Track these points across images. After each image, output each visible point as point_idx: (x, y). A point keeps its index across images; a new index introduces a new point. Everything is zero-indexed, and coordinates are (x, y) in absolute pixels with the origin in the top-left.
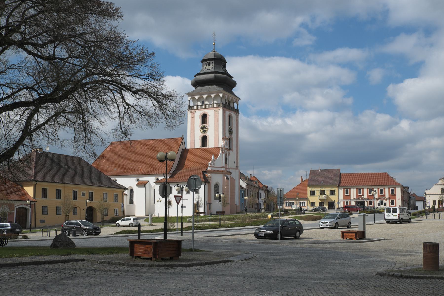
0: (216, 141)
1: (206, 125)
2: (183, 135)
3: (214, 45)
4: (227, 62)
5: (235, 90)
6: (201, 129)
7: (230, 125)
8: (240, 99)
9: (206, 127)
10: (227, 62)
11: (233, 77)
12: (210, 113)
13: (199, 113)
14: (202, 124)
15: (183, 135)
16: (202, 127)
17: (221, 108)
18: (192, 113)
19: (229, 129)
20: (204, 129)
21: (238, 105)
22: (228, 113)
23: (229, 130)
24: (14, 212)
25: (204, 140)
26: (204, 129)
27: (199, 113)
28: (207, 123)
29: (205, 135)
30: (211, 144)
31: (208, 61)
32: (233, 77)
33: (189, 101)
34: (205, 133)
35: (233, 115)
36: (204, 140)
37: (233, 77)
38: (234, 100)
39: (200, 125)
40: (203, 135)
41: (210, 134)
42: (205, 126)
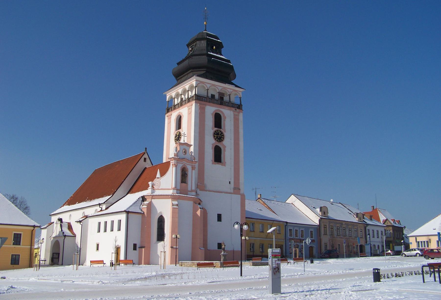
9: (222, 133)
16: (215, 132)
24: (360, 253)
28: (221, 128)
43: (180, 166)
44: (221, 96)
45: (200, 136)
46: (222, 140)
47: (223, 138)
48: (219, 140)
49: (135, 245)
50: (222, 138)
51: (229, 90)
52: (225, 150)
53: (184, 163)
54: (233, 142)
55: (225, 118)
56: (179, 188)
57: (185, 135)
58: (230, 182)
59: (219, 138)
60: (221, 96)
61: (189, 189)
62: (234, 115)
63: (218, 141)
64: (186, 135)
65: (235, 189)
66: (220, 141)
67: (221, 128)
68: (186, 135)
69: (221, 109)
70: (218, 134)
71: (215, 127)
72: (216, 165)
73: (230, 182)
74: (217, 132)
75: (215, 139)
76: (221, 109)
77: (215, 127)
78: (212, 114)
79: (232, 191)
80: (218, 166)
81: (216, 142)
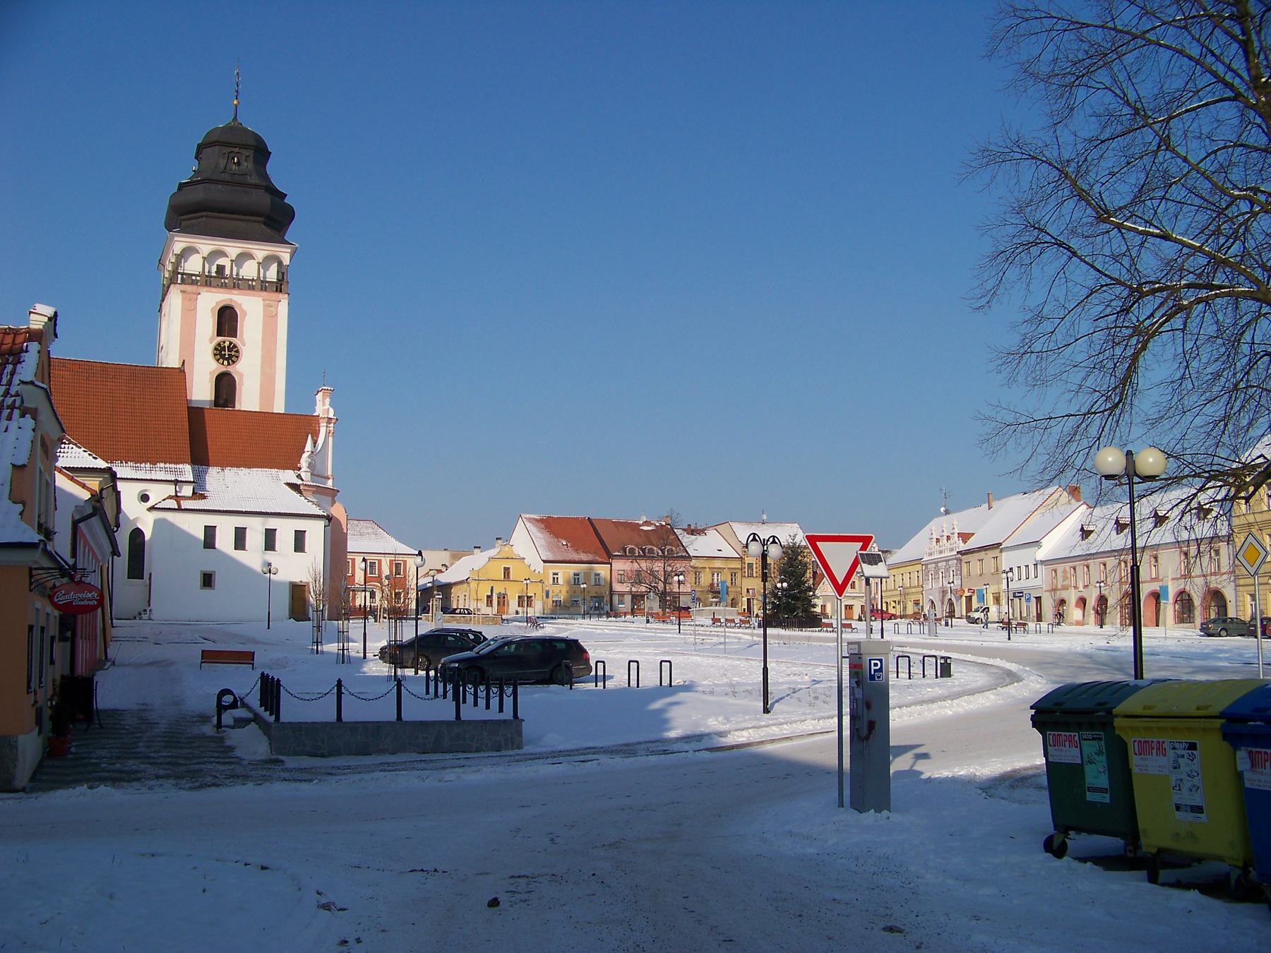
0: (267, 389)
2: (184, 362)
6: (216, 349)
9: (235, 346)
12: (250, 307)
13: (210, 301)
15: (184, 362)
18: (185, 295)
20: (227, 354)
25: (225, 387)
26: (227, 354)
27: (210, 301)
29: (230, 369)
30: (248, 399)
31: (233, 149)
34: (229, 364)
36: (225, 387)
39: (211, 341)
40: (223, 369)
41: (247, 371)
42: (231, 343)
46: (234, 362)
47: (237, 357)
48: (226, 362)
52: (241, 380)
55: (245, 314)
59: (227, 356)
62: (266, 306)
66: (229, 364)
71: (219, 335)
75: (218, 360)
77: (219, 335)
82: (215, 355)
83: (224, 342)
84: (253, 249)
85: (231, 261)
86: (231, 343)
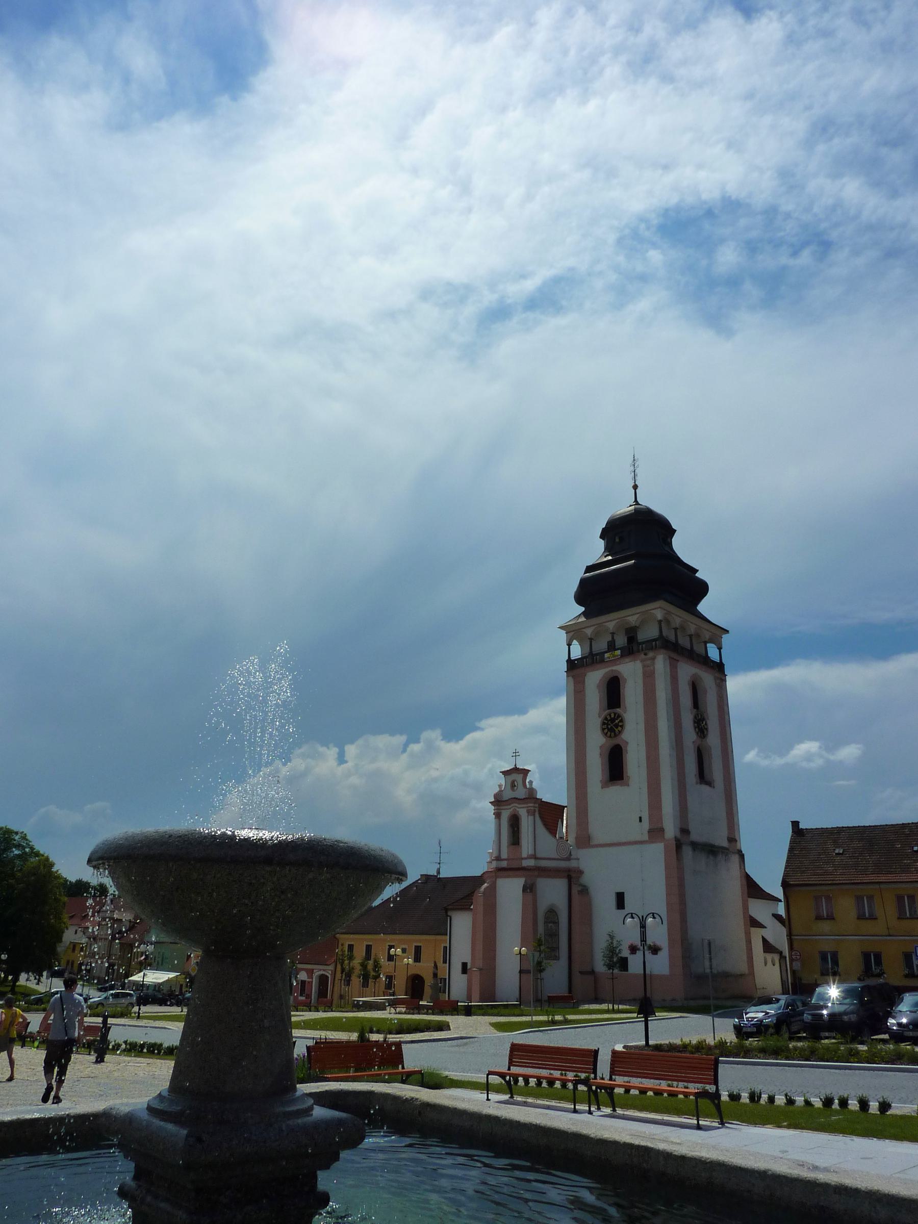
1: (618, 709)
3: (635, 487)
4: (676, 531)
5: (704, 607)
6: (604, 724)
7: (696, 704)
8: (727, 632)
9: (619, 716)
10: (676, 531)
11: (697, 571)
13: (595, 678)
14: (609, 709)
16: (606, 719)
17: (662, 651)
19: (695, 717)
21: (720, 649)
22: (687, 671)
23: (695, 722)
28: (619, 706)
32: (698, 571)
33: (569, 645)
35: (707, 679)
37: (697, 571)
38: (707, 635)
43: (506, 815)
44: (631, 633)
45: (576, 739)
49: (464, 965)
50: (619, 727)
51: (630, 619)
53: (513, 807)
54: (642, 726)
56: (504, 855)
57: (517, 754)
58: (640, 818)
60: (631, 633)
61: (524, 855)
63: (610, 737)
64: (518, 752)
65: (650, 831)
66: (616, 735)
67: (619, 706)
68: (518, 752)
69: (614, 668)
70: (613, 720)
72: (611, 788)
73: (640, 818)
74: (609, 718)
75: (606, 734)
76: (614, 668)
78: (598, 686)
79: (646, 837)
80: (615, 790)
81: (609, 739)
82: (603, 729)
83: (610, 716)
84: (626, 617)
85: (611, 633)
86: (615, 714)
